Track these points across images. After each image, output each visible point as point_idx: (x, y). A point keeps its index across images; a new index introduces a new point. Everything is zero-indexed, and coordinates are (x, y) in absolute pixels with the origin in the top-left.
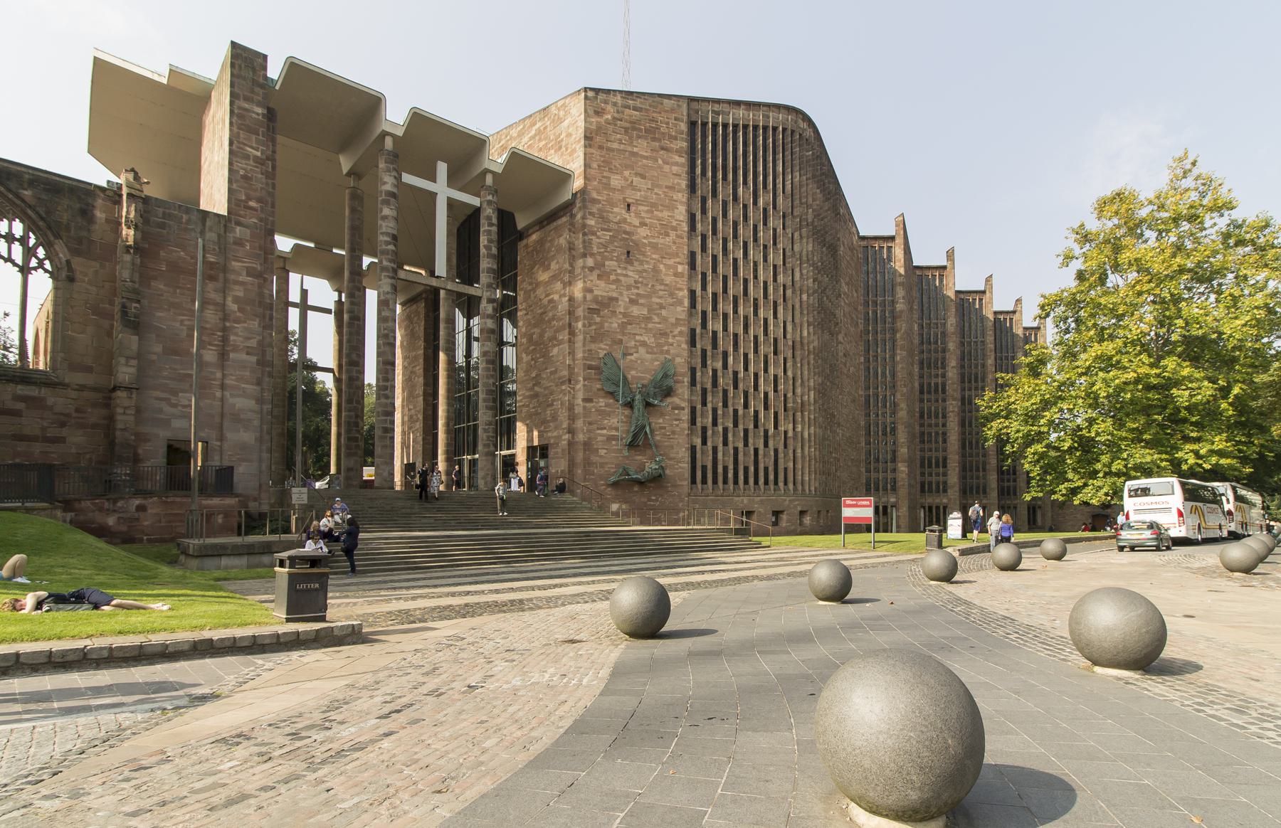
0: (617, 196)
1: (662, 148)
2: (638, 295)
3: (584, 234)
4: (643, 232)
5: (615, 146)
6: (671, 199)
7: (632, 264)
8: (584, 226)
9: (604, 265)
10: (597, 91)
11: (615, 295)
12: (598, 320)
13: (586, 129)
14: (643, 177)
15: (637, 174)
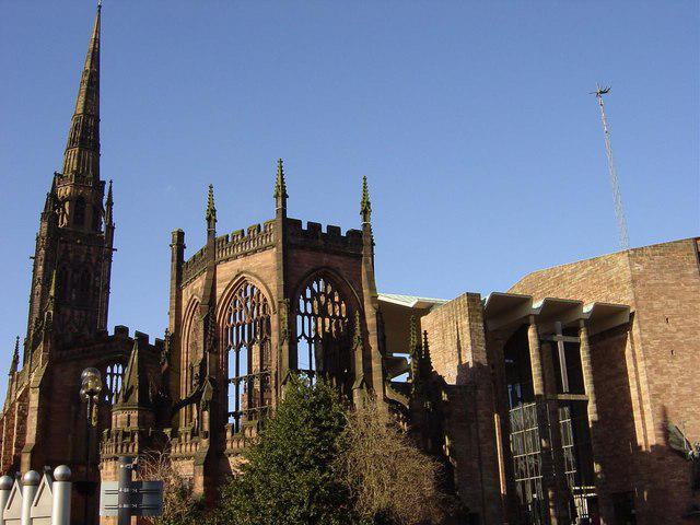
0: (659, 315)
1: (682, 276)
2: (683, 379)
3: (642, 345)
4: (680, 335)
5: (653, 282)
6: (695, 309)
7: (674, 358)
8: (642, 339)
9: (657, 363)
10: (635, 250)
11: (668, 382)
12: (660, 401)
13: (633, 276)
14: (673, 298)
15: (670, 297)
